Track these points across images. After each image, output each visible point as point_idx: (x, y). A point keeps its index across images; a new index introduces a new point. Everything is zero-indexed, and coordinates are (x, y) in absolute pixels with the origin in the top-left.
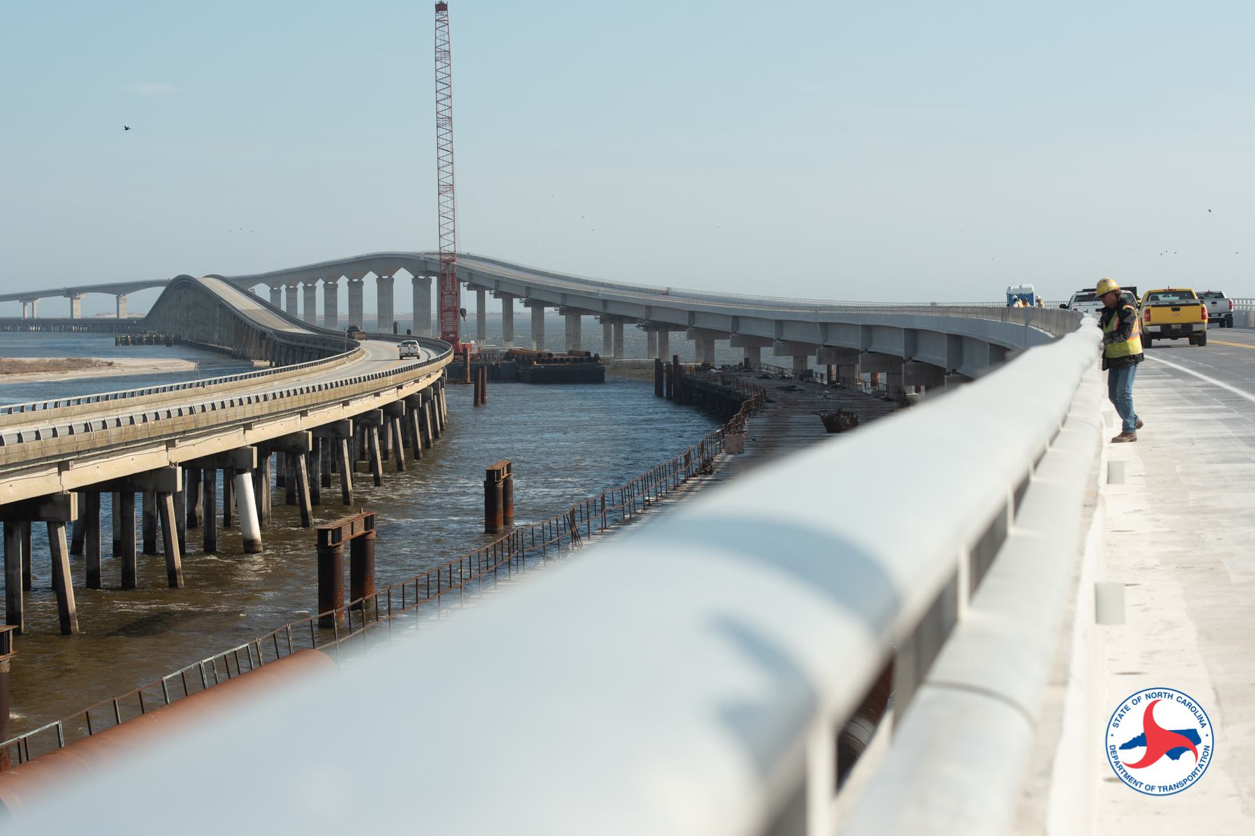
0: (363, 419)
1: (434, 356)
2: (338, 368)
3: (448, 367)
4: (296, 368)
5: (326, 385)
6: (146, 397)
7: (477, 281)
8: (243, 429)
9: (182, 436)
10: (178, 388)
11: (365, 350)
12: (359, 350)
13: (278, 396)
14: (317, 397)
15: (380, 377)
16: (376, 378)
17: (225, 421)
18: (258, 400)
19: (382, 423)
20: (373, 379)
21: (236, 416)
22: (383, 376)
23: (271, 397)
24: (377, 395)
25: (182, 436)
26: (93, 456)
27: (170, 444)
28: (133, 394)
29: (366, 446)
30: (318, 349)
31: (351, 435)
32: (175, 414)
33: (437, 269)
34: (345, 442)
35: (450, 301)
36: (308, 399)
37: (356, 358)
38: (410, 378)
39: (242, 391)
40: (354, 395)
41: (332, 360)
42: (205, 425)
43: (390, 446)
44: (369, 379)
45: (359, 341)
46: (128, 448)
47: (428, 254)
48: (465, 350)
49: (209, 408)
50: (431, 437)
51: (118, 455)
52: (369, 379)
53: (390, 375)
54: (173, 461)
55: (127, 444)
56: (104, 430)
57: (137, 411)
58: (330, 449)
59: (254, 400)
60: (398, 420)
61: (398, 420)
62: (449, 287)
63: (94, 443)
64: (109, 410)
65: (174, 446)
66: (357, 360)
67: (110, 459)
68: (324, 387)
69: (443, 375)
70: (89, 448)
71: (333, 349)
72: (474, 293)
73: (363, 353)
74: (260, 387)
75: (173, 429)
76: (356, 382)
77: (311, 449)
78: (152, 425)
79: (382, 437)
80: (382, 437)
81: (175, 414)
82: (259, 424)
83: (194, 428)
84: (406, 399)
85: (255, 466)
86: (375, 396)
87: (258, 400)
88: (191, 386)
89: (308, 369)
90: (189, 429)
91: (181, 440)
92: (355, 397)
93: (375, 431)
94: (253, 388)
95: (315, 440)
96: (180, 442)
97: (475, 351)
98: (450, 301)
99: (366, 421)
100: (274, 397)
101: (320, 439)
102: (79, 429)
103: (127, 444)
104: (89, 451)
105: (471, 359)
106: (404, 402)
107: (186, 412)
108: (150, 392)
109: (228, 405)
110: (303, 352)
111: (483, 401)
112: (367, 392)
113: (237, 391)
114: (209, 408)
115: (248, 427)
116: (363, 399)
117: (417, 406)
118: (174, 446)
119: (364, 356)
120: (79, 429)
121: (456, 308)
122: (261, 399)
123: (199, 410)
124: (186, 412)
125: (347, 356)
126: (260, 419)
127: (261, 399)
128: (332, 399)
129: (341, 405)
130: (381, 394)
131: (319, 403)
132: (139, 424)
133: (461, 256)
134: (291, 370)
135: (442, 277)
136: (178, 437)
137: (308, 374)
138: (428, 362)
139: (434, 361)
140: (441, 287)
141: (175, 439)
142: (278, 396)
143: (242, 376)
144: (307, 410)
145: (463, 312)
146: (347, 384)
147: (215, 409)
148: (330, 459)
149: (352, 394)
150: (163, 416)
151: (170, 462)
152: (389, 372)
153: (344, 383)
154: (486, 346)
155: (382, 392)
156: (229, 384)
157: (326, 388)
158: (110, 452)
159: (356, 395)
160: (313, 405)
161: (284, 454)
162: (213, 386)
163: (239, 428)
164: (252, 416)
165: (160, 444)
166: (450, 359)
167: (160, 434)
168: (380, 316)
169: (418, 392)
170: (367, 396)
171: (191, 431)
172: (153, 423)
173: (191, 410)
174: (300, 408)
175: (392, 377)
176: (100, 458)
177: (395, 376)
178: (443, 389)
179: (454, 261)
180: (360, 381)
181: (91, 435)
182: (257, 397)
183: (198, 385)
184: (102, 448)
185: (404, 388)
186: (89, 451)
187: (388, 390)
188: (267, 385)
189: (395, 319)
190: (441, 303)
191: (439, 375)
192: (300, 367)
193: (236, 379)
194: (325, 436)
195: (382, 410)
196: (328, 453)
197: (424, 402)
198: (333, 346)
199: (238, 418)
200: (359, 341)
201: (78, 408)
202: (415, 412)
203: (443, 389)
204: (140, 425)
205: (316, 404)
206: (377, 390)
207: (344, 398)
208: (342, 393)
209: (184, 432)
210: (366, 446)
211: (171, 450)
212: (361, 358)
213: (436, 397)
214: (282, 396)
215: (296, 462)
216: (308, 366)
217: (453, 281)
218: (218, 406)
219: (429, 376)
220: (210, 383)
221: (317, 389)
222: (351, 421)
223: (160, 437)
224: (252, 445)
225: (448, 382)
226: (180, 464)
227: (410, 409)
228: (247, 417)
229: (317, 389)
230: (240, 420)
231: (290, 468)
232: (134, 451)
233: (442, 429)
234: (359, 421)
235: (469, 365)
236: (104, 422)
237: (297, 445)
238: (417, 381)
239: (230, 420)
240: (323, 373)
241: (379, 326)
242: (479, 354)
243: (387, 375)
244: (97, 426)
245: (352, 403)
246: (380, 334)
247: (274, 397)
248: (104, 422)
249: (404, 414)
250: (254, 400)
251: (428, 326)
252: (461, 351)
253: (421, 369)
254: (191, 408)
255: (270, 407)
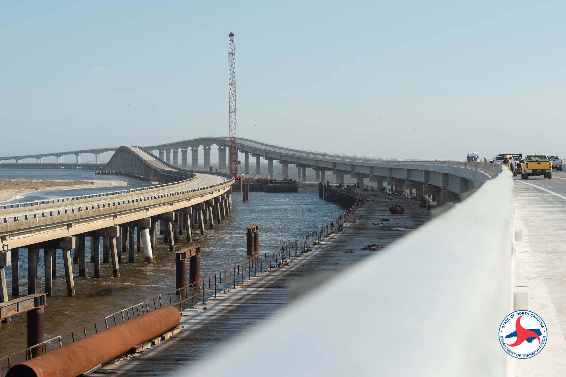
0: (196, 207)
1: (226, 180)
2: (186, 185)
3: (232, 185)
5: (181, 192)
6: (105, 197)
7: (245, 149)
8: (145, 210)
9: (119, 213)
10: (119, 193)
11: (198, 177)
18: (152, 198)
19: (204, 209)
20: (200, 190)
21: (143, 205)
23: (157, 197)
24: (202, 196)
25: (119, 213)
26: (82, 221)
27: (115, 217)
28: (100, 196)
29: (198, 218)
31: (191, 213)
32: (117, 204)
33: (229, 144)
34: (188, 216)
35: (234, 158)
37: (194, 181)
38: (216, 190)
39: (146, 194)
40: (192, 197)
41: (184, 182)
42: (129, 209)
43: (208, 218)
44: (199, 190)
45: (195, 174)
46: (97, 218)
47: (225, 138)
48: (240, 178)
49: (131, 202)
50: (225, 215)
51: (92, 221)
54: (116, 224)
55: (96, 216)
56: (87, 211)
57: (101, 203)
58: (182, 220)
59: (150, 199)
60: (211, 207)
61: (211, 207)
62: (233, 152)
63: (83, 216)
64: (89, 202)
65: (116, 217)
66: (195, 182)
67: (89, 222)
68: (180, 193)
69: (230, 188)
70: (80, 218)
71: (185, 177)
72: (244, 154)
73: (197, 179)
74: (153, 193)
75: (116, 210)
76: (193, 191)
77: (174, 219)
78: (107, 209)
79: (205, 214)
80: (205, 214)
81: (117, 204)
83: (125, 210)
84: (215, 198)
85: (150, 226)
87: (152, 198)
88: (124, 192)
89: (174, 186)
91: (119, 215)
92: (193, 197)
93: (201, 212)
94: (151, 193)
95: (176, 215)
97: (244, 179)
98: (234, 158)
99: (197, 207)
100: (159, 197)
102: (76, 210)
103: (96, 216)
104: (80, 219)
105: (242, 182)
107: (121, 203)
108: (107, 195)
109: (139, 200)
110: (172, 178)
111: (247, 200)
112: (198, 195)
114: (131, 202)
115: (147, 210)
117: (219, 202)
118: (116, 217)
119: (198, 180)
120: (76, 210)
121: (236, 160)
122: (153, 198)
123: (127, 202)
124: (121, 203)
125: (190, 180)
126: (152, 206)
127: (153, 198)
128: (183, 198)
129: (187, 201)
130: (204, 196)
131: (178, 200)
132: (101, 208)
133: (239, 139)
135: (231, 148)
136: (118, 213)
138: (224, 183)
139: (226, 183)
140: (230, 152)
141: (117, 215)
145: (239, 162)
148: (182, 223)
149: (192, 196)
150: (112, 205)
151: (115, 224)
154: (249, 176)
155: (204, 195)
156: (140, 191)
157: (181, 193)
158: (89, 220)
159: (193, 196)
160: (175, 201)
161: (163, 221)
162: (133, 192)
165: (111, 216)
166: (233, 182)
167: (110, 213)
168: (205, 164)
170: (198, 197)
171: (123, 211)
172: (108, 208)
173: (124, 203)
174: (170, 202)
175: (209, 189)
176: (85, 222)
178: (230, 194)
179: (235, 141)
180: (195, 191)
181: (81, 212)
184: (86, 218)
185: (214, 194)
186: (80, 219)
188: (156, 192)
189: (211, 165)
190: (230, 158)
191: (229, 188)
192: (170, 185)
196: (181, 221)
197: (222, 200)
199: (143, 206)
200: (195, 174)
201: (77, 201)
203: (230, 194)
204: (102, 208)
205: (176, 200)
207: (188, 198)
208: (187, 196)
209: (121, 212)
210: (198, 218)
211: (115, 219)
212: (196, 181)
213: (227, 198)
215: (168, 224)
216: (174, 184)
217: (235, 149)
218: (135, 201)
219: (224, 189)
220: (132, 191)
221: (177, 194)
222: (191, 207)
223: (110, 214)
224: (149, 217)
225: (233, 191)
226: (119, 225)
228: (147, 205)
229: (177, 194)
230: (144, 207)
231: (165, 227)
232: (99, 220)
233: (229, 211)
234: (195, 207)
235: (241, 184)
236: (87, 207)
238: (219, 191)
241: (204, 168)
242: (246, 180)
244: (84, 209)
245: (192, 200)
246: (205, 171)
247: (159, 197)
248: (87, 207)
250: (150, 199)
251: (225, 168)
252: (238, 178)
253: (221, 186)
254: (123, 202)
255: (157, 201)
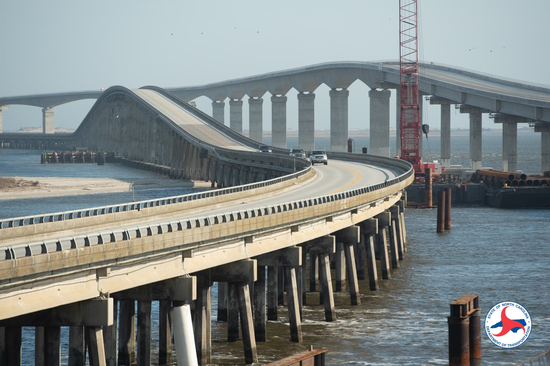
0: (313, 246)
1: (392, 176)
2: (286, 190)
4: (241, 189)
5: (273, 208)
8: (181, 256)
9: (114, 264)
12: (309, 170)
13: (220, 220)
14: (263, 222)
15: (332, 200)
16: (328, 201)
17: (162, 248)
18: (198, 225)
19: (334, 251)
20: (324, 202)
22: (336, 199)
23: (212, 221)
24: (329, 219)
25: (114, 264)
30: (265, 169)
31: (300, 263)
32: (106, 239)
34: (293, 271)
36: (253, 224)
37: (306, 179)
38: (365, 201)
40: (304, 220)
41: (279, 181)
42: (140, 252)
44: (320, 202)
49: (144, 233)
52: (320, 202)
53: (344, 197)
59: (193, 225)
60: (352, 248)
61: (352, 248)
66: (308, 181)
68: (270, 211)
71: (281, 169)
73: (314, 173)
74: (200, 210)
75: (105, 256)
76: (306, 205)
77: (255, 279)
80: (335, 266)
81: (106, 239)
82: (198, 251)
83: (127, 255)
84: (361, 224)
85: (194, 297)
86: (327, 221)
87: (198, 225)
89: (253, 191)
90: (122, 256)
91: (113, 268)
92: (305, 221)
93: (327, 259)
94: (193, 212)
95: (261, 269)
96: (111, 270)
99: (316, 248)
100: (216, 221)
101: (266, 267)
106: (359, 227)
107: (119, 237)
109: (165, 229)
110: (247, 172)
112: (318, 217)
113: (175, 215)
114: (144, 233)
115: (186, 254)
116: (313, 224)
119: (315, 176)
122: (202, 223)
124: (119, 237)
125: (296, 176)
126: (200, 245)
127: (202, 223)
128: (279, 224)
129: (290, 230)
130: (334, 219)
131: (266, 229)
134: (234, 191)
136: (110, 265)
137: (253, 196)
142: (220, 220)
143: (181, 198)
144: (252, 236)
146: (296, 207)
147: (151, 235)
149: (302, 218)
152: (343, 194)
153: (293, 206)
155: (334, 216)
156: (166, 207)
157: (274, 211)
159: (306, 220)
160: (259, 230)
162: (149, 209)
163: (178, 255)
164: (191, 242)
168: (333, 133)
169: (374, 217)
170: (318, 221)
171: (124, 258)
173: (125, 236)
174: (245, 233)
175: (346, 200)
177: (348, 199)
182: (197, 221)
183: (132, 208)
185: (359, 212)
187: (341, 214)
188: (208, 208)
189: (350, 136)
192: (245, 189)
193: (174, 201)
194: (271, 265)
195: (334, 237)
197: (381, 228)
198: (281, 165)
199: (177, 244)
202: (371, 239)
205: (262, 230)
206: (329, 214)
207: (292, 223)
209: (117, 260)
212: (312, 179)
214: (224, 220)
216: (253, 187)
218: (154, 231)
220: (145, 205)
221: (263, 212)
222: (300, 249)
224: (192, 274)
226: (112, 295)
227: (365, 236)
228: (186, 243)
229: (263, 212)
230: (179, 247)
234: (309, 248)
237: (241, 274)
238: (373, 205)
239: (167, 246)
240: (270, 195)
241: (332, 143)
243: (340, 198)
245: (301, 229)
246: (333, 153)
247: (216, 221)
249: (359, 241)
250: (193, 225)
251: (386, 144)
253: (377, 191)
254: (124, 233)
255: (211, 232)
